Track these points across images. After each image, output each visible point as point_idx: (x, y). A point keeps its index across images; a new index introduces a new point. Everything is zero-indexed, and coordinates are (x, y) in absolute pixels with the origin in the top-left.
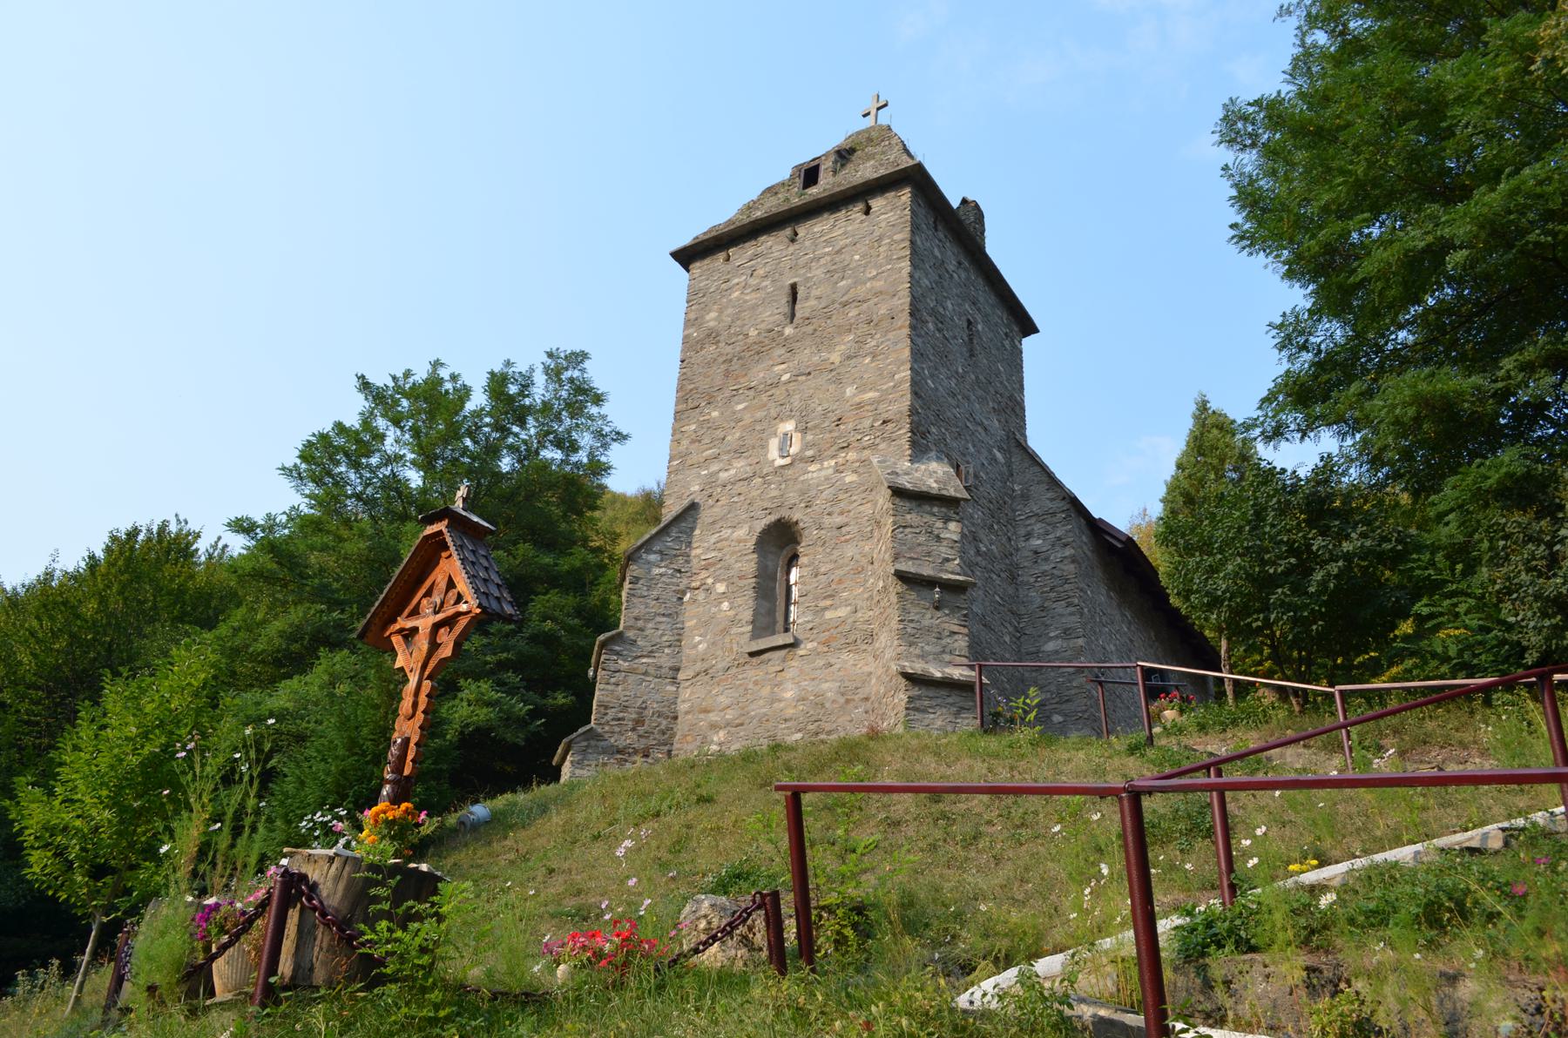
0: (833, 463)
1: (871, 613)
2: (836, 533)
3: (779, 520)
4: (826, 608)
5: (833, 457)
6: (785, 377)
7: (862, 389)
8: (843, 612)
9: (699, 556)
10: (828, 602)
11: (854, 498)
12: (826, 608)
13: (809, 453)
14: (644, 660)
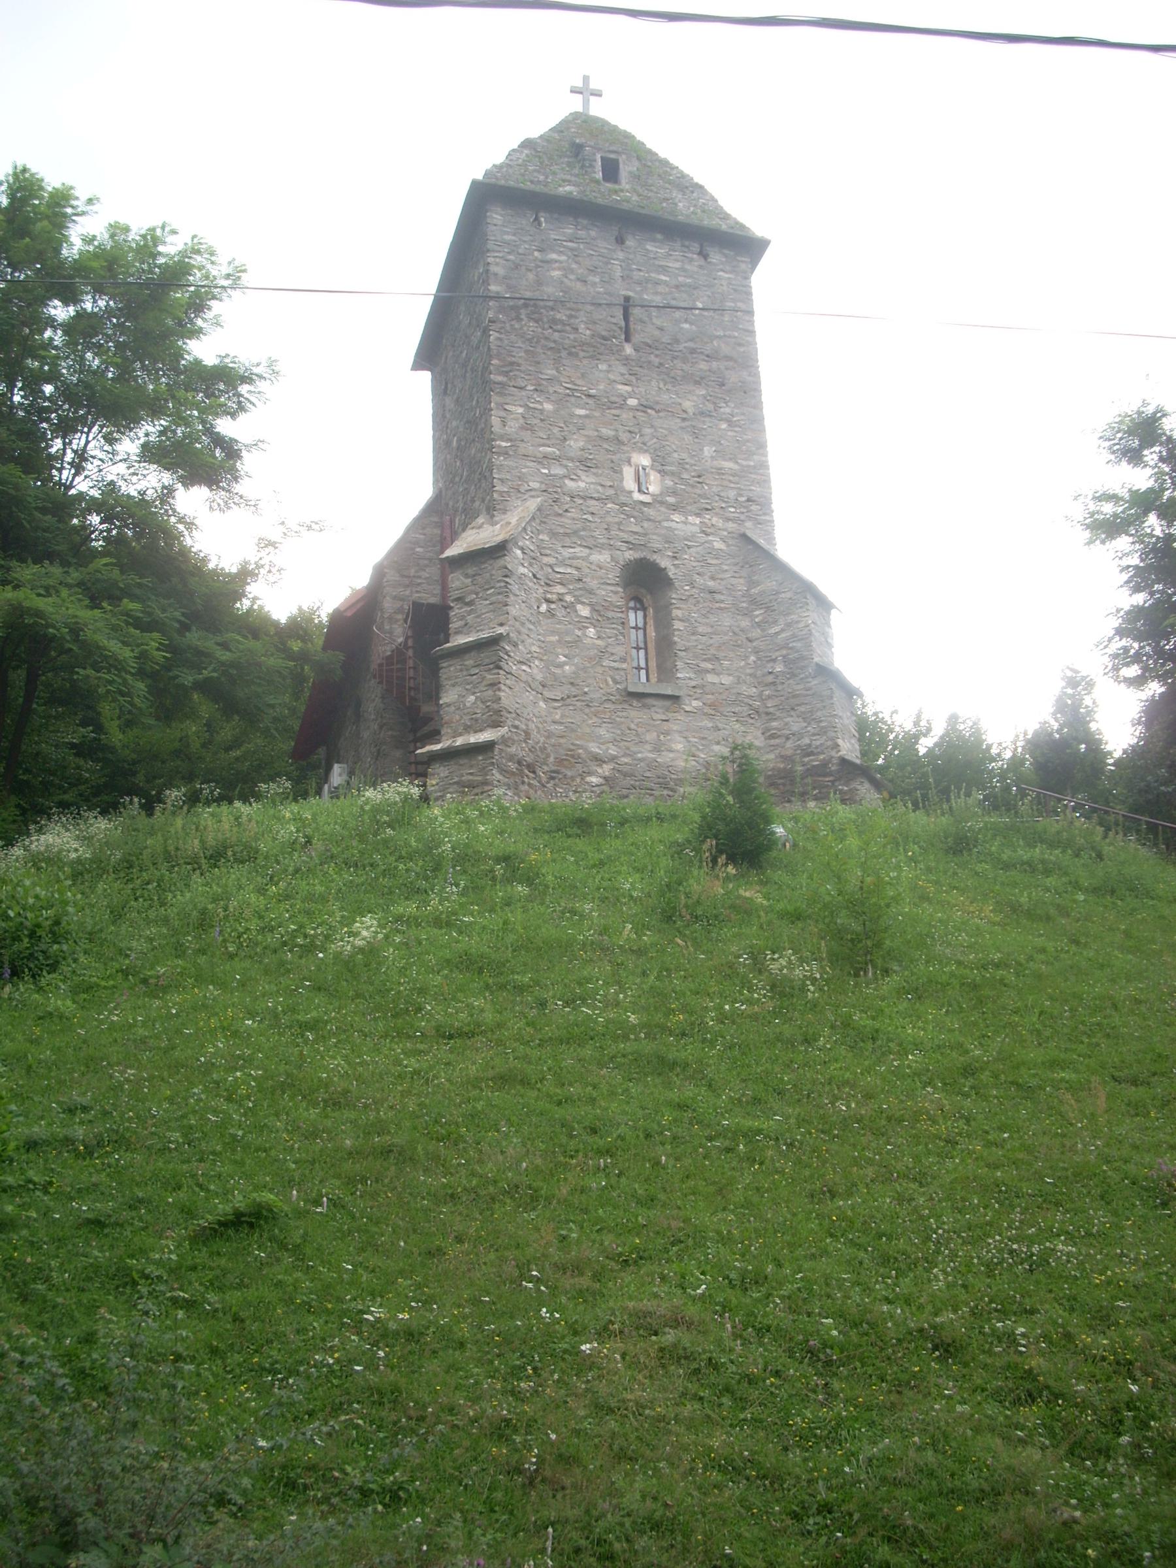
0: (698, 521)
1: (754, 690)
2: (708, 596)
3: (641, 559)
4: (708, 671)
5: (698, 515)
6: (632, 402)
7: (720, 453)
8: (727, 680)
9: (551, 566)
10: (710, 666)
11: (726, 567)
12: (708, 671)
13: (671, 500)
14: (524, 667)
